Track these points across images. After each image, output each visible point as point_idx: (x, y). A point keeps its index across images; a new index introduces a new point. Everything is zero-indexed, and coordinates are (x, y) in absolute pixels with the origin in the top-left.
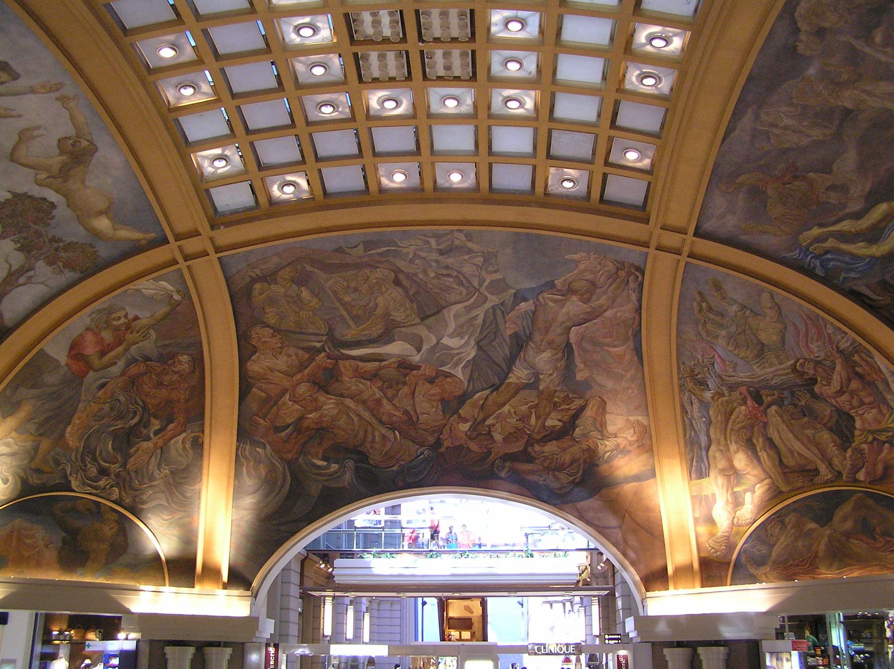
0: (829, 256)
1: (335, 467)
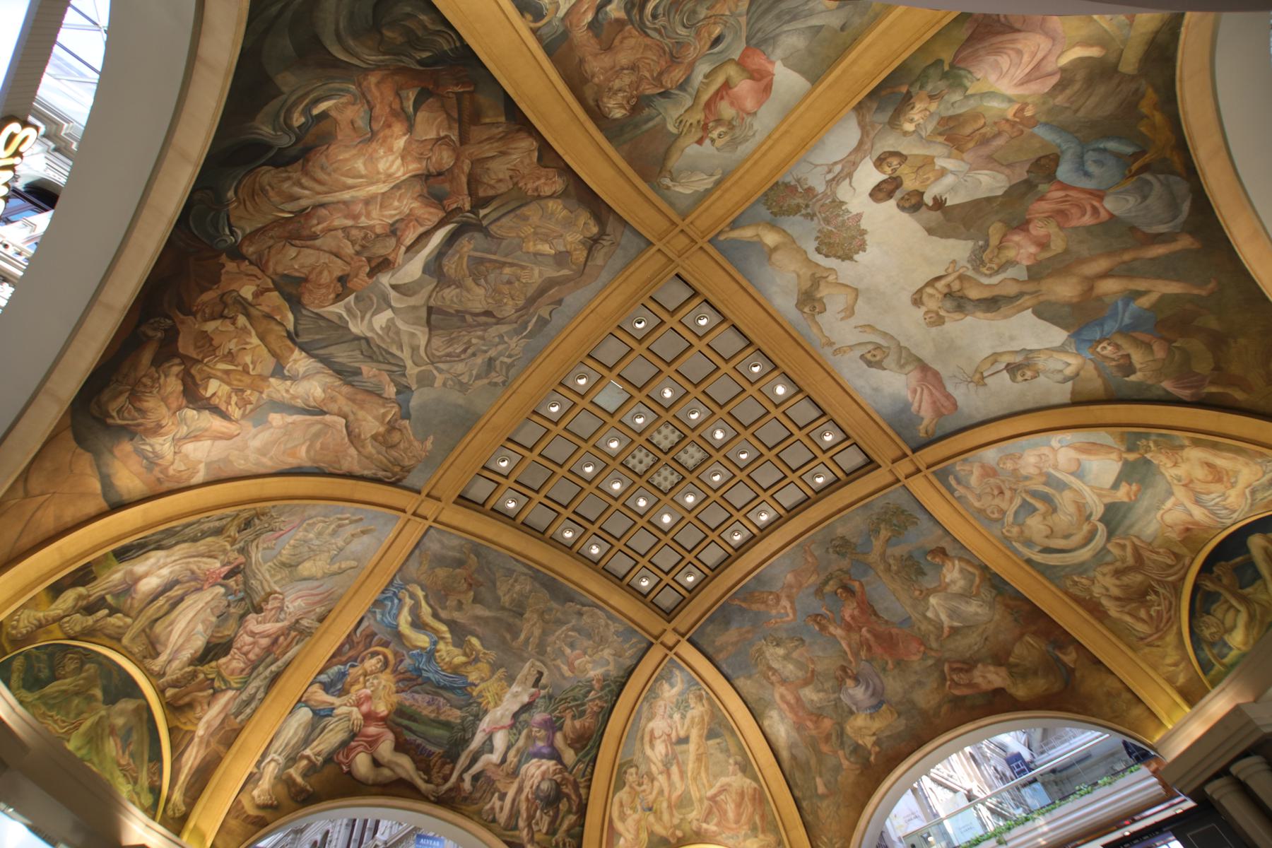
0: (396, 601)
1: (298, 120)
